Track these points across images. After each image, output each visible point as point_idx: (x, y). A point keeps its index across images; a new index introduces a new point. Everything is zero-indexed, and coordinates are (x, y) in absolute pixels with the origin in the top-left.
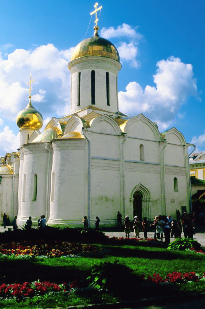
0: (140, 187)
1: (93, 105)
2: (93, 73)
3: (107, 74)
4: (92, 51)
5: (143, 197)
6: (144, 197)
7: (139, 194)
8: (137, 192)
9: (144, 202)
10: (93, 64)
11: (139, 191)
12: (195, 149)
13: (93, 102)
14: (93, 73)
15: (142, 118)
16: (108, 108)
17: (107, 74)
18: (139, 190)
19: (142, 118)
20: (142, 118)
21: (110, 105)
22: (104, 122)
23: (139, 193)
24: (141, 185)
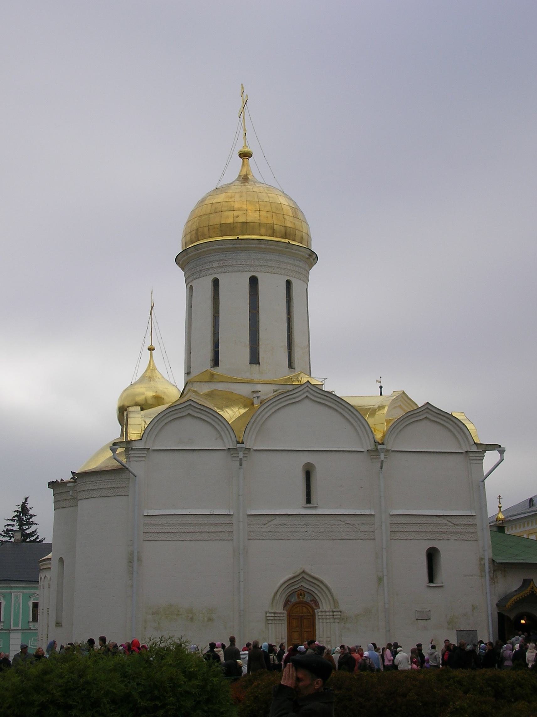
0: (303, 577)
1: (216, 371)
2: (216, 283)
3: (254, 281)
4: (207, 228)
5: (318, 607)
6: (321, 607)
7: (307, 599)
8: (301, 593)
9: (321, 621)
10: (213, 261)
11: (303, 588)
12: (502, 460)
13: (216, 362)
14: (216, 283)
15: (310, 393)
16: (254, 372)
17: (254, 281)
18: (302, 586)
19: (312, 392)
20: (310, 393)
21: (259, 363)
22: (189, 420)
23: (306, 595)
24: (304, 572)
